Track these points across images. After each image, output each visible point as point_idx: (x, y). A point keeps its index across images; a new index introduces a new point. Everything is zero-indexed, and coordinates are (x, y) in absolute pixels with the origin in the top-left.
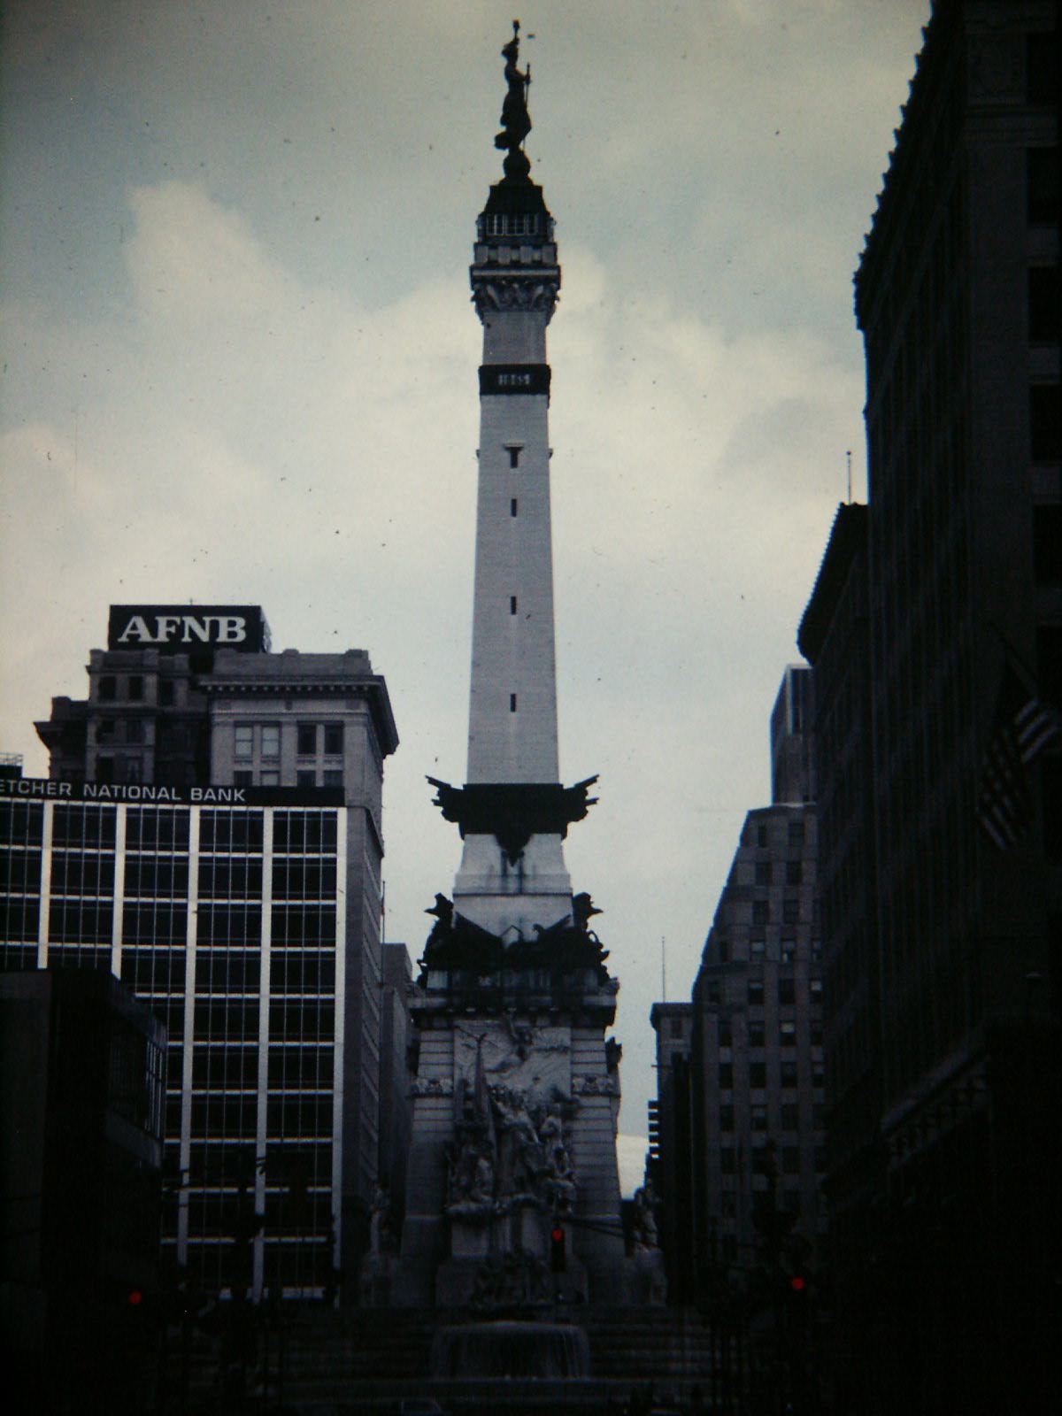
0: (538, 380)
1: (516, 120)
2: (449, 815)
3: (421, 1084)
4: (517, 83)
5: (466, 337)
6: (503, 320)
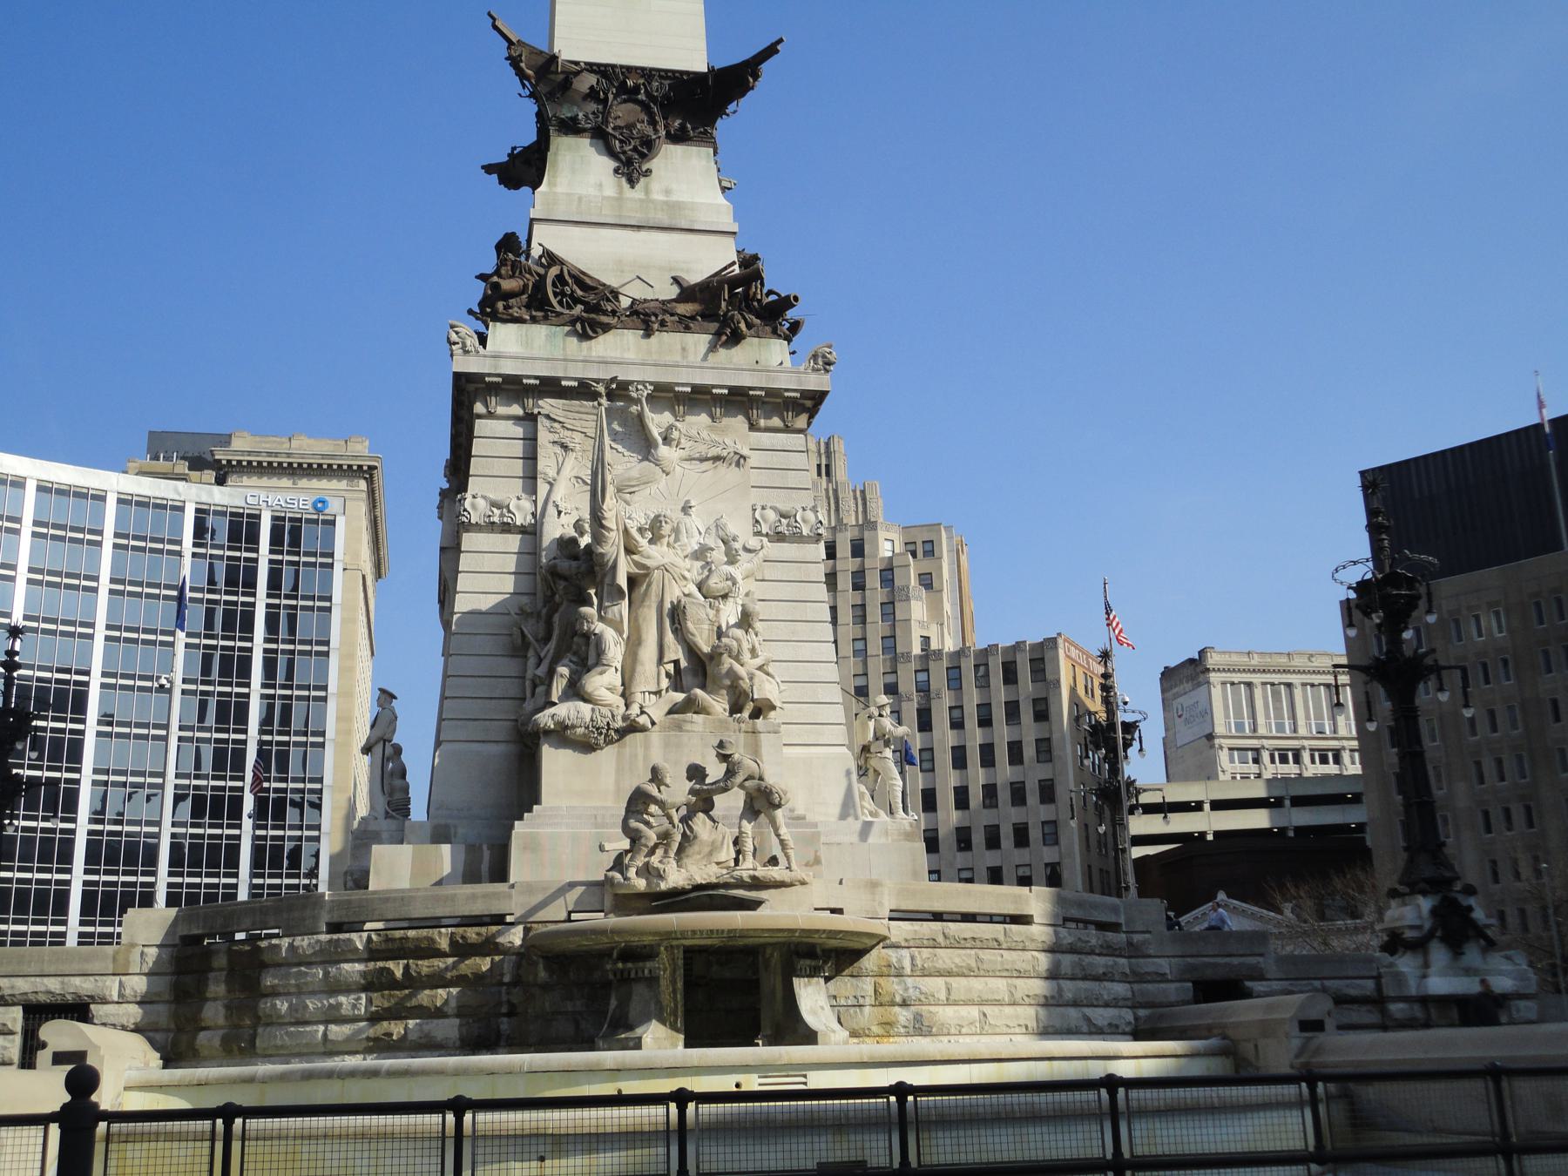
3: (473, 506)
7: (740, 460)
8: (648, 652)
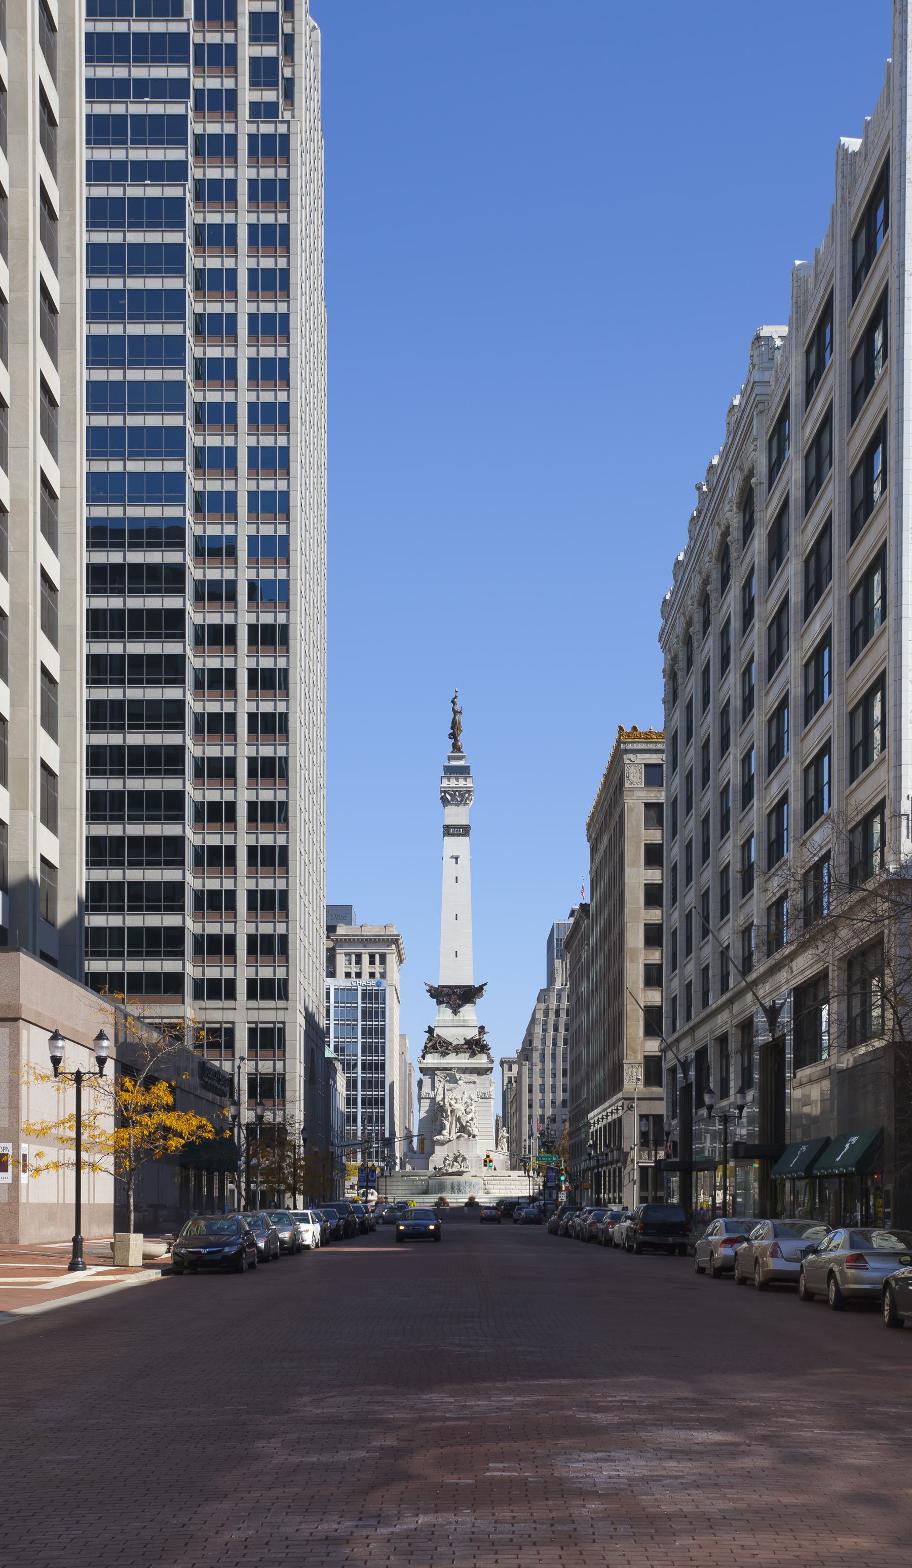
2: (432, 996)
7: (474, 1082)
8: (454, 1126)
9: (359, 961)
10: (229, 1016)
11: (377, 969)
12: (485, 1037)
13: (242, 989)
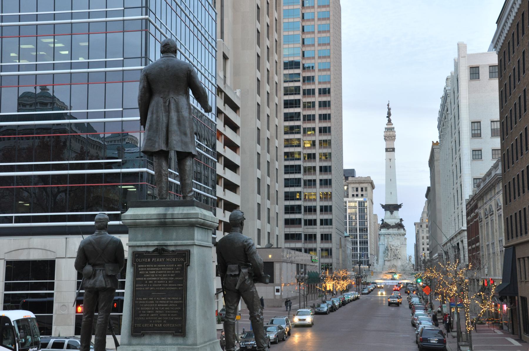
0: (393, 150)
1: (389, 114)
2: (383, 208)
4: (389, 109)
5: (383, 145)
6: (388, 142)
9: (357, 190)
10: (315, 230)
11: (364, 193)
12: (403, 222)
13: (318, 222)
